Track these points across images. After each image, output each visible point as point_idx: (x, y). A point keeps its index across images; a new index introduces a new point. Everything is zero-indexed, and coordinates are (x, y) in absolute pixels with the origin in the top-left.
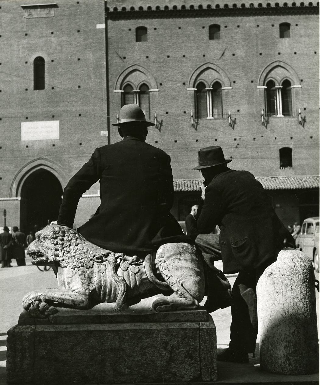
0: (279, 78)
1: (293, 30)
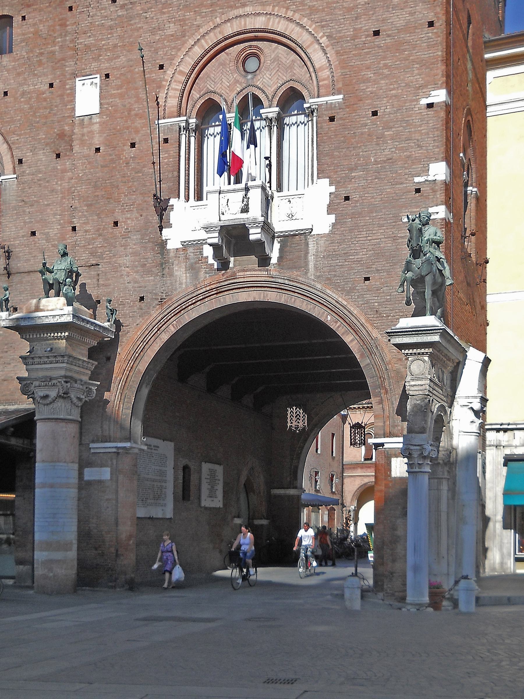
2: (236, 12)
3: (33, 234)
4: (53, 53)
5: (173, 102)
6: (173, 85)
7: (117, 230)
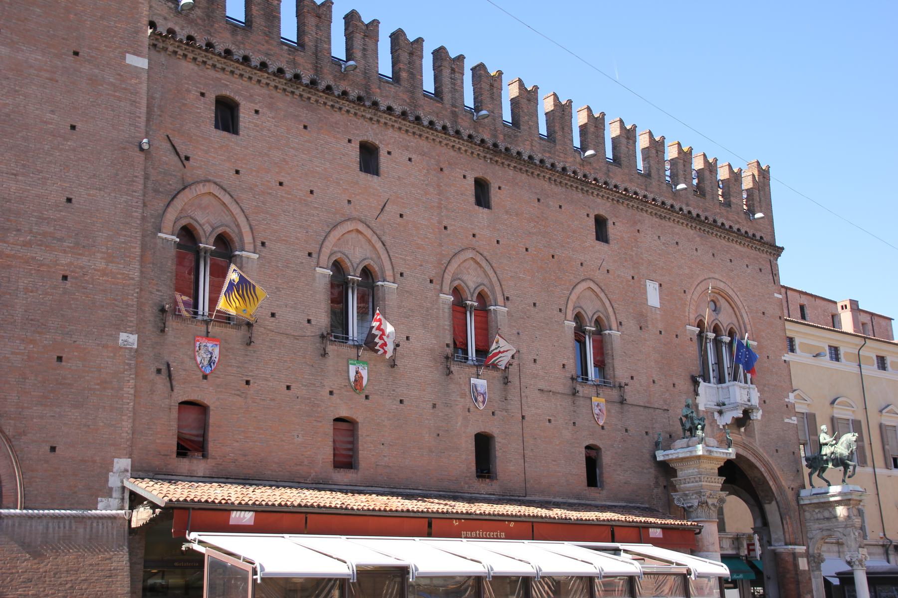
0: (472, 285)
5: (692, 317)
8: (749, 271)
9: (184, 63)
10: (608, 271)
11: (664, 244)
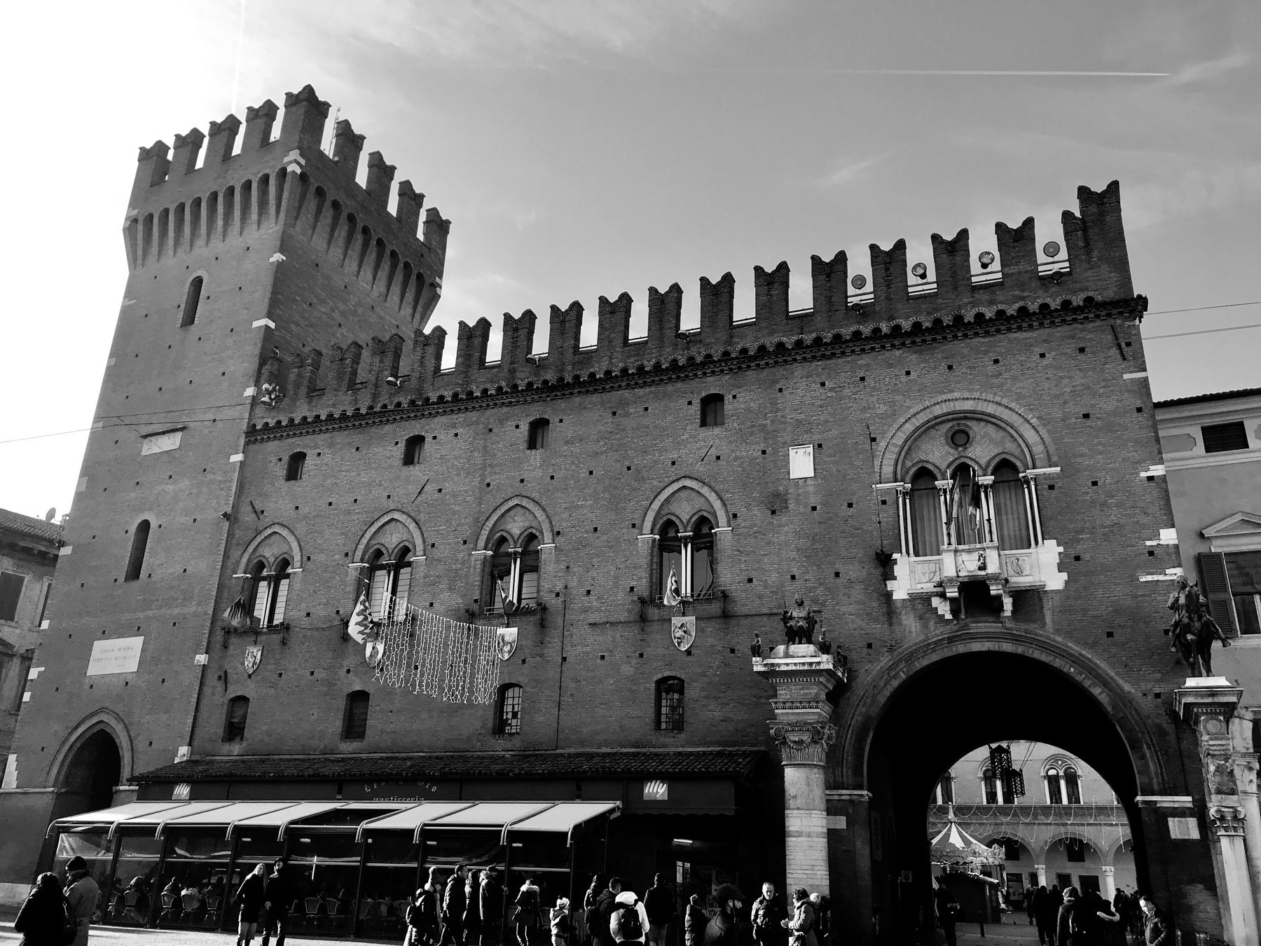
0: (516, 531)
1: (556, 432)
2: (945, 397)
3: (750, 580)
4: (765, 426)
5: (888, 470)
6: (887, 455)
7: (838, 580)
8: (1045, 362)
9: (270, 443)
10: (718, 458)
11: (831, 390)
